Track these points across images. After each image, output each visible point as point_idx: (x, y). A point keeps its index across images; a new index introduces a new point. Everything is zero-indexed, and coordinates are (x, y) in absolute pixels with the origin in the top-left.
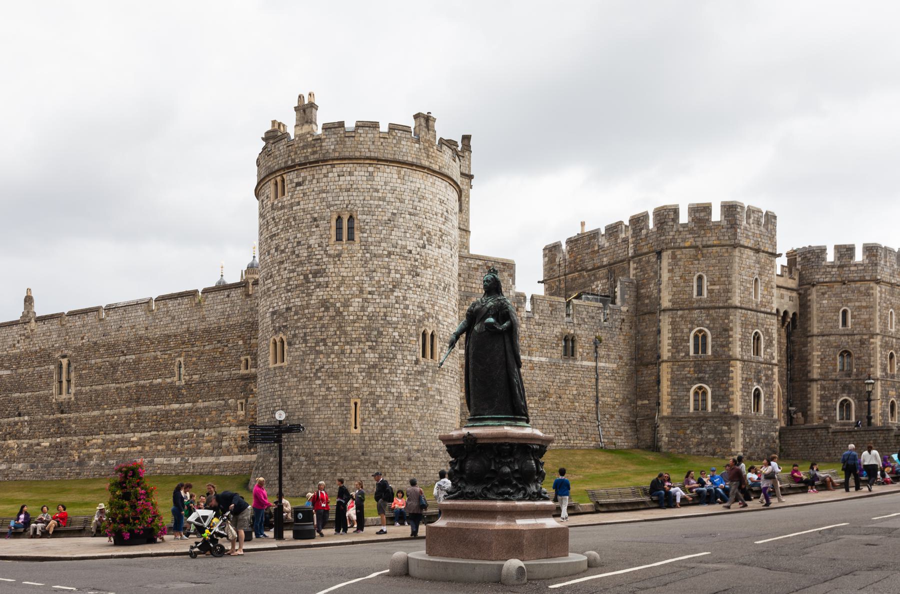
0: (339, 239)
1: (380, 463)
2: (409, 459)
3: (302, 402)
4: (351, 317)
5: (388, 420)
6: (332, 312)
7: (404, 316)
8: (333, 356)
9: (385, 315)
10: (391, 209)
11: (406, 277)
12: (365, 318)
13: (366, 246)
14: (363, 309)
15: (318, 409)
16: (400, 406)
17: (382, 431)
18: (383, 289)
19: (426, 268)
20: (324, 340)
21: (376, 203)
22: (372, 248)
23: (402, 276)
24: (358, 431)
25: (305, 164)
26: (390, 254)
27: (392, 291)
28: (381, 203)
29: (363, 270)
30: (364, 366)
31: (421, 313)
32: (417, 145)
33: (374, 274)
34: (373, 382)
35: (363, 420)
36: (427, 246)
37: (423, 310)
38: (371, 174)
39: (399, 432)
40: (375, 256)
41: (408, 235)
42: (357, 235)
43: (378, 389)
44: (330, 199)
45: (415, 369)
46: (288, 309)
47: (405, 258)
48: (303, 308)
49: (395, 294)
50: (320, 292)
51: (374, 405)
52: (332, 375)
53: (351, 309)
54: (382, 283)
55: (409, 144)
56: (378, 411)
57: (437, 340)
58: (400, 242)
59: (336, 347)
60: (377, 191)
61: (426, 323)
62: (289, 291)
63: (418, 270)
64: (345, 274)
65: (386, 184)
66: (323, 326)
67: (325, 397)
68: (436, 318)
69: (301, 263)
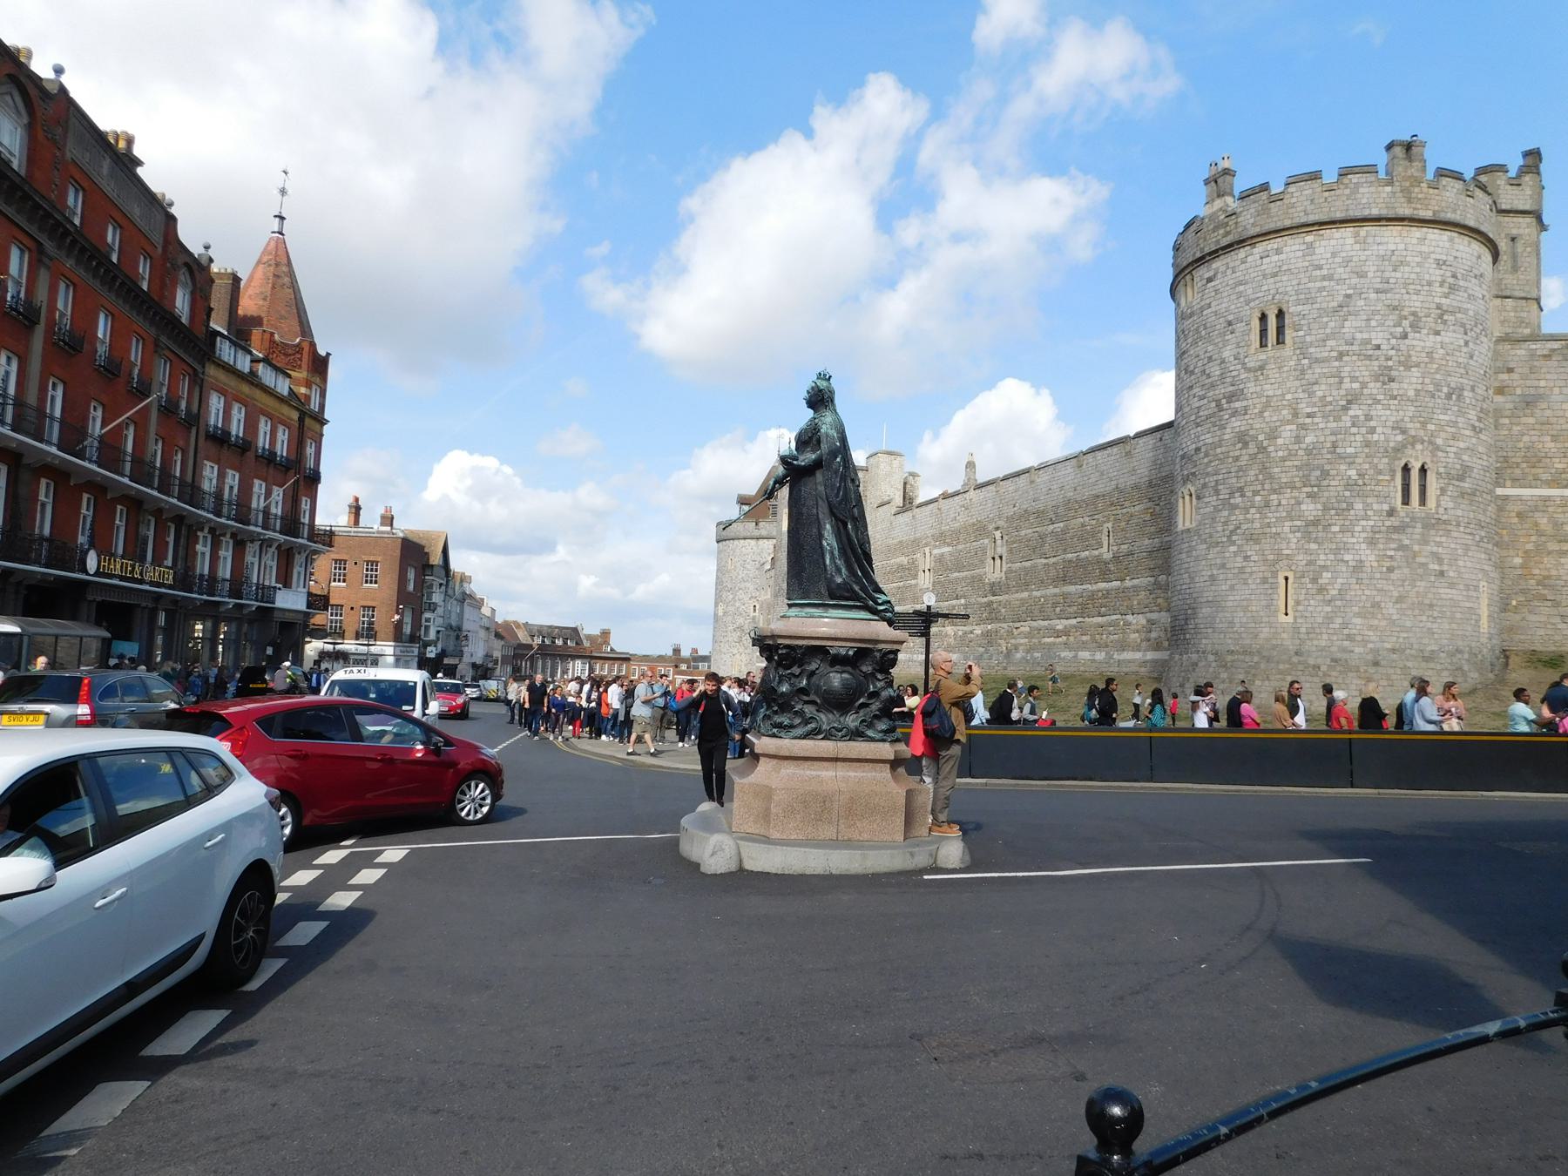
0: (1263, 344)
1: (1324, 668)
2: (1376, 664)
3: (1213, 578)
4: (1280, 454)
5: (1339, 603)
6: (1252, 449)
7: (1367, 444)
8: (1253, 511)
9: (1334, 446)
10: (1343, 290)
11: (1371, 385)
12: (1301, 452)
13: (1302, 350)
14: (1298, 440)
15: (1232, 588)
16: (1359, 581)
17: (1329, 619)
18: (1329, 408)
19: (1408, 368)
20: (1241, 490)
21: (1318, 284)
22: (1312, 350)
23: (1364, 385)
24: (1290, 619)
25: (1216, 251)
26: (1341, 355)
27: (1345, 409)
28: (1326, 283)
29: (1297, 383)
30: (1298, 523)
31: (1400, 438)
32: (1389, 189)
33: (1316, 388)
34: (1313, 546)
35: (1298, 603)
36: (1411, 335)
37: (1404, 432)
38: (1310, 246)
39: (1358, 621)
40: (1317, 361)
41: (1373, 323)
42: (1289, 334)
43: (1322, 557)
44: (1250, 292)
45: (1388, 523)
46: (1198, 450)
47: (1369, 358)
48: (1215, 446)
49: (1351, 413)
50: (1237, 424)
51: (1314, 580)
52: (1252, 538)
53: (1280, 441)
54: (1329, 399)
55: (1373, 189)
56: (1321, 590)
57: (1431, 477)
58: (1358, 336)
59: (1258, 498)
60: (1320, 268)
61: (1409, 451)
62: (1198, 425)
63: (1394, 373)
64: (1271, 393)
65: (1334, 255)
66: (1240, 469)
67: (1242, 570)
68: (1430, 443)
69: (1213, 386)
